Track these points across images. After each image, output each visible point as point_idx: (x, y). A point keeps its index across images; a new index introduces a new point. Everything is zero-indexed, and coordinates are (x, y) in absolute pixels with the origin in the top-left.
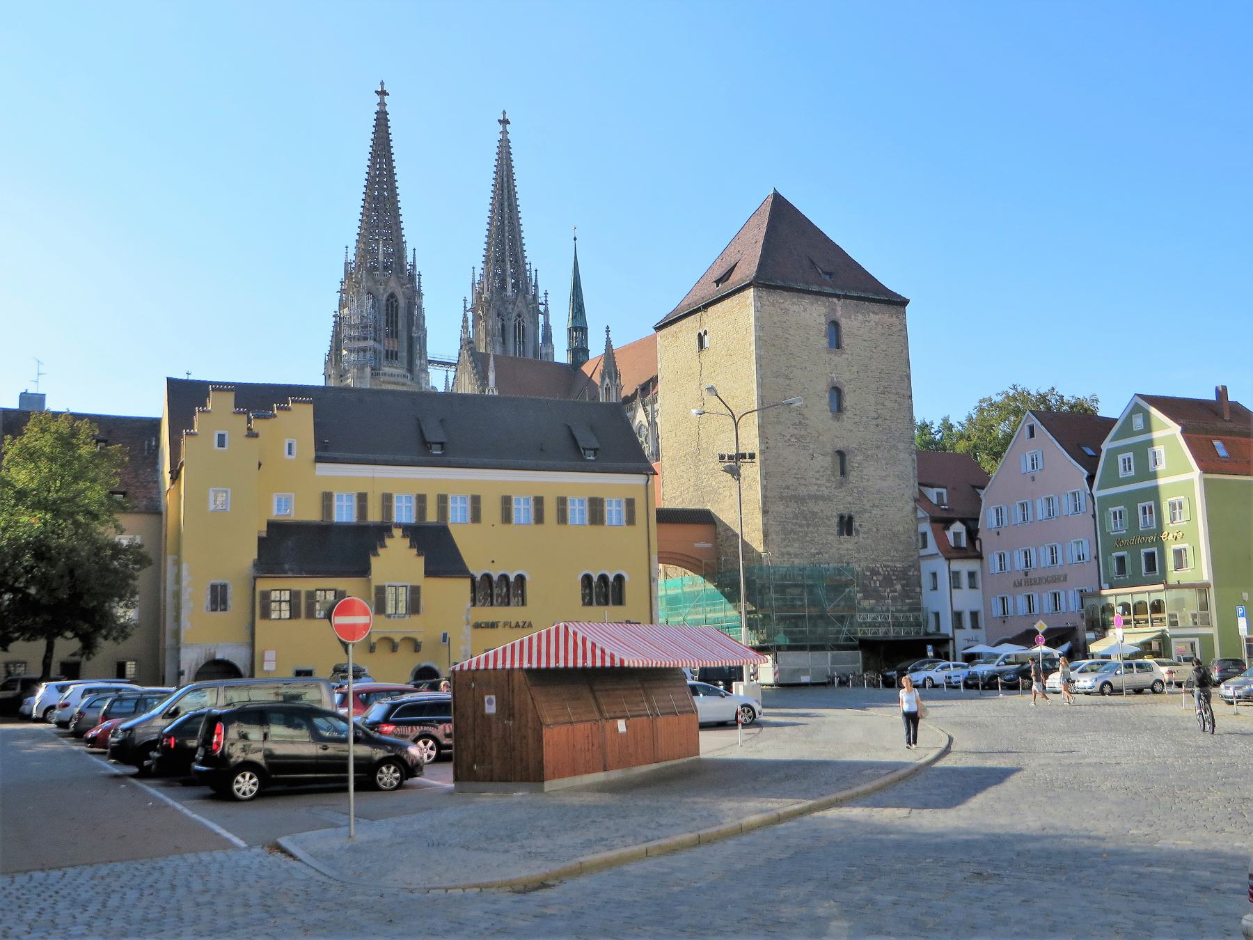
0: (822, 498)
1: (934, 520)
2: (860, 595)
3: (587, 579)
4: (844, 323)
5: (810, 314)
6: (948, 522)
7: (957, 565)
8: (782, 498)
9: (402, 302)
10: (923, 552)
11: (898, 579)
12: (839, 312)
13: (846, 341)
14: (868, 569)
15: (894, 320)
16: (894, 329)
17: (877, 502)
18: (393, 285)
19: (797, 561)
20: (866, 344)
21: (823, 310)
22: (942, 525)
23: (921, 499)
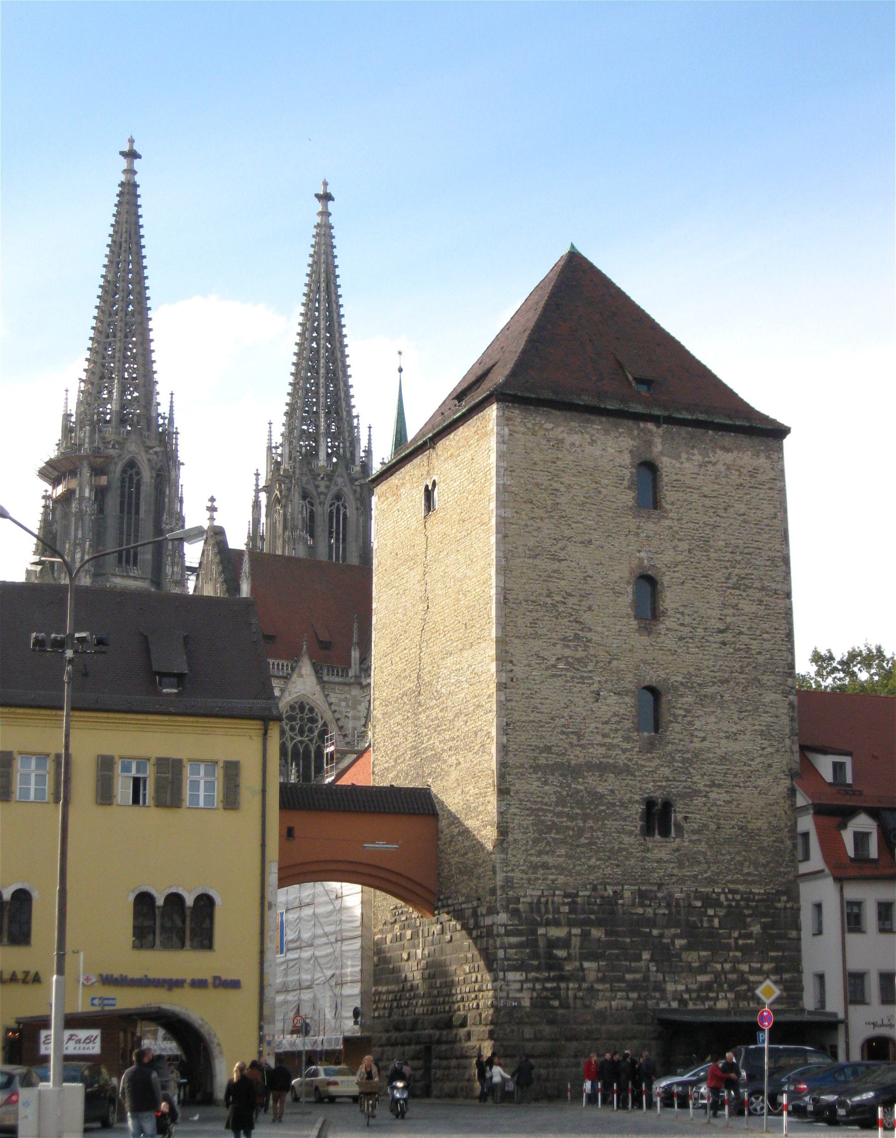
1: (820, 811)
2: (679, 942)
3: (144, 900)
4: (666, 463)
5: (607, 449)
6: (845, 814)
7: (853, 892)
8: (536, 768)
9: (147, 476)
10: (804, 868)
12: (658, 446)
13: (669, 496)
14: (698, 896)
15: (762, 461)
16: (761, 478)
17: (719, 779)
18: (133, 448)
19: (561, 879)
20: (707, 502)
21: (627, 443)
22: (833, 821)
23: (804, 772)
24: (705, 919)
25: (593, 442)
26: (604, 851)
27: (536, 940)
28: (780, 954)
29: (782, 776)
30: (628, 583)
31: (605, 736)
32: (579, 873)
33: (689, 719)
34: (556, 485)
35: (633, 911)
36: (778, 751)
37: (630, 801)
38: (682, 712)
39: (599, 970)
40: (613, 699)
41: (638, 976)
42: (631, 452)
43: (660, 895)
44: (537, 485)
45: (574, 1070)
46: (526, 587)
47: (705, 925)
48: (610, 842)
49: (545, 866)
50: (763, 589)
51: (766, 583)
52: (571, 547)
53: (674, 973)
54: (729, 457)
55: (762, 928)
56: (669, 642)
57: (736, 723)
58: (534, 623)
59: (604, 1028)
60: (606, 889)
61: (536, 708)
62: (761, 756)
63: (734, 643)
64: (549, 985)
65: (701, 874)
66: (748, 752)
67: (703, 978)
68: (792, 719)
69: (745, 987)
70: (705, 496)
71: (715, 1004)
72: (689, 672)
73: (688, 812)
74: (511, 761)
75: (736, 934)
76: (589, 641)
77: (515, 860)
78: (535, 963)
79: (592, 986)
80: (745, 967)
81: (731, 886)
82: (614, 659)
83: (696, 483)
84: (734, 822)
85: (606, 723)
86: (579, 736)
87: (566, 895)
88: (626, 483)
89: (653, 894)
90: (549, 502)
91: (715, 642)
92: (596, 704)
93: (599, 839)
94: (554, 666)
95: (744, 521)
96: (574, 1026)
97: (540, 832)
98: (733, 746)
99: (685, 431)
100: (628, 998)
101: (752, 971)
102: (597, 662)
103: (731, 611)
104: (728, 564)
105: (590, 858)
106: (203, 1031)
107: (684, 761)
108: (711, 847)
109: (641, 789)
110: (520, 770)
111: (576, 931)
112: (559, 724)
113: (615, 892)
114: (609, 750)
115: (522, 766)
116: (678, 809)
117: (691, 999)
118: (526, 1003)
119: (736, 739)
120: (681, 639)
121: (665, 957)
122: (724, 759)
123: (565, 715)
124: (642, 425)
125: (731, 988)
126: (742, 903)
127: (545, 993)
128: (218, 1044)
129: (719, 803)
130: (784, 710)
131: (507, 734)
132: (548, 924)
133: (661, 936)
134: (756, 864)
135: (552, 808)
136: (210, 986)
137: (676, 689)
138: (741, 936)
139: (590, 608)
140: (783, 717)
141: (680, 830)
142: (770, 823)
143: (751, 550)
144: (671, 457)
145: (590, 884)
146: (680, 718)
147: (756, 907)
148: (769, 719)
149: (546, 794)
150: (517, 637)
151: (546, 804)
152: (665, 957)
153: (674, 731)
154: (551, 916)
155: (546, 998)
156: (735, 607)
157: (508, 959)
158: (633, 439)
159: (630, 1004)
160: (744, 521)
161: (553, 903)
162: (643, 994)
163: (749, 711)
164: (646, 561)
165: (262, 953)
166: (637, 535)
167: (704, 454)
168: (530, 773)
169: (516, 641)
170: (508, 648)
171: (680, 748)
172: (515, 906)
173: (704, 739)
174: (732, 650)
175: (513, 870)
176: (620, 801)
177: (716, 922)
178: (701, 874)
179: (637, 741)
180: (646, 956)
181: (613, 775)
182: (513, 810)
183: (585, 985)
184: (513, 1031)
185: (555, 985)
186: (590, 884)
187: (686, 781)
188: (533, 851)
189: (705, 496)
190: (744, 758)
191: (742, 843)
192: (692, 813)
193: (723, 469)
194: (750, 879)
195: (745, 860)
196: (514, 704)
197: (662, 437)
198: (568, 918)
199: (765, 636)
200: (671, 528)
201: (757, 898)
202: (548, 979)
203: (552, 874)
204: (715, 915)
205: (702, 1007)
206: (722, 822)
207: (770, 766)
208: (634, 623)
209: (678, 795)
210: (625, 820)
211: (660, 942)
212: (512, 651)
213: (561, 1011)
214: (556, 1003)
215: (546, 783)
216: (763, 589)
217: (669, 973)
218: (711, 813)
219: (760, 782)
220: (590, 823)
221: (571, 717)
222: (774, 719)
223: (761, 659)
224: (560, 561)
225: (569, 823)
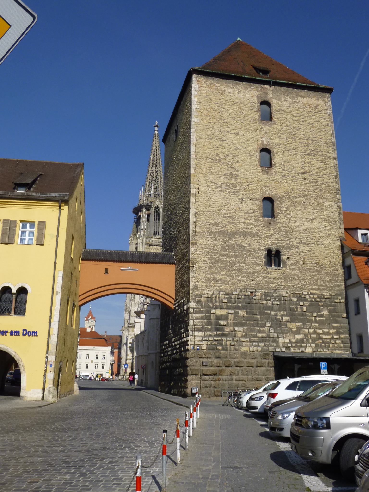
0: (251, 234)
2: (285, 318)
4: (274, 102)
8: (211, 233)
11: (326, 305)
13: (276, 115)
14: (295, 295)
16: (320, 109)
17: (304, 240)
19: (223, 286)
20: (294, 118)
24: (299, 307)
25: (239, 92)
26: (246, 273)
27: (210, 316)
28: (339, 325)
29: (336, 239)
30: (257, 151)
31: (245, 219)
32: (233, 284)
33: (288, 212)
34: (221, 109)
35: (261, 302)
36: (333, 228)
37: (259, 250)
38: (284, 209)
39: (243, 332)
40: (249, 202)
41: (264, 335)
42: (257, 97)
43: (275, 295)
44: (212, 109)
45: (230, 382)
46: (206, 152)
47: (299, 310)
48: (249, 269)
49: (215, 280)
50: (323, 155)
51: (324, 153)
52: (228, 135)
53: (283, 333)
54: (305, 100)
55: (328, 312)
56: (278, 178)
57: (312, 215)
58: (210, 168)
59: (246, 361)
60: (247, 292)
61: (211, 205)
62: (325, 230)
63: (309, 179)
64: (216, 339)
65: (296, 285)
66: (318, 228)
67: (299, 336)
68: (340, 214)
69: (321, 341)
70: (293, 116)
71: (305, 350)
72: (287, 191)
73: (287, 255)
74: (198, 230)
75: (315, 315)
76: (238, 176)
77: (199, 276)
78: (210, 327)
79: (240, 339)
80: (320, 331)
81: (312, 291)
82: (250, 184)
83: (290, 110)
84: (312, 261)
85: (246, 213)
86: (233, 219)
87: (226, 294)
88: (255, 109)
89: (271, 294)
90: (218, 116)
91: (300, 178)
92: (241, 204)
93: (243, 267)
94: (220, 187)
95: (313, 127)
96: (230, 360)
97: (213, 263)
98: (310, 225)
99: (283, 89)
100: (259, 346)
101: (324, 333)
102: (242, 185)
103: (308, 165)
104: (305, 145)
105: (238, 276)
106: (16, 358)
107: (286, 231)
108: (301, 272)
109: (264, 244)
110: (203, 234)
111: (231, 311)
112: (222, 213)
113: (252, 293)
114: (248, 225)
115: (203, 232)
116: (283, 254)
117: (292, 346)
118: (204, 347)
119: (312, 222)
120: (283, 176)
121: (278, 325)
122: (306, 231)
123: (226, 209)
124: (262, 86)
125: (313, 342)
126: (318, 299)
127: (214, 343)
128: (23, 366)
129: (304, 251)
130: (335, 210)
131: (196, 217)
132: (216, 308)
133: (276, 315)
134: (324, 281)
135: (219, 252)
136: (21, 334)
137: (281, 199)
138: (318, 316)
139: (238, 162)
140: (335, 213)
141: (285, 263)
142: (330, 261)
143: (317, 139)
144: (276, 99)
145: (238, 289)
146: (283, 212)
147: (325, 302)
148: (328, 213)
149: (216, 245)
150: (201, 173)
151: (216, 250)
152: (278, 325)
153: (280, 217)
154: (218, 304)
155: (215, 345)
156: (310, 163)
157: (195, 325)
158: (258, 91)
159: (260, 349)
160: (313, 127)
161: (219, 297)
162: (267, 344)
163: (318, 209)
164: (265, 142)
165: (51, 317)
166: (261, 131)
167: (293, 98)
168: (208, 236)
169: (201, 175)
170: (197, 178)
171: (284, 225)
172: (199, 299)
173: (296, 222)
174: (308, 182)
175: (198, 281)
176: (254, 249)
177: (305, 309)
178: (296, 285)
179: (262, 222)
180: (268, 324)
181: (250, 237)
182: (198, 252)
183: (236, 339)
184: (197, 361)
185: (220, 338)
186: (238, 289)
187: (287, 241)
188: (209, 272)
189: (293, 116)
190: (316, 231)
191: (317, 270)
192: (291, 256)
193: (302, 105)
194: (321, 288)
195: (319, 279)
196: (199, 203)
197: (272, 91)
198: (227, 305)
199: (325, 176)
200: (277, 128)
201: (325, 297)
202: (215, 336)
203: (219, 283)
204: (304, 305)
205: (298, 351)
206: (306, 260)
207: (329, 235)
208: (260, 169)
209: (283, 247)
210: (256, 258)
211: (276, 318)
212: (199, 179)
213: (222, 352)
214: (220, 348)
215: (215, 240)
216: (323, 155)
217: (280, 333)
218: (300, 256)
219: (325, 242)
220: (238, 259)
221: (228, 210)
222: (331, 213)
223: (323, 186)
224: (223, 141)
225: (227, 259)
